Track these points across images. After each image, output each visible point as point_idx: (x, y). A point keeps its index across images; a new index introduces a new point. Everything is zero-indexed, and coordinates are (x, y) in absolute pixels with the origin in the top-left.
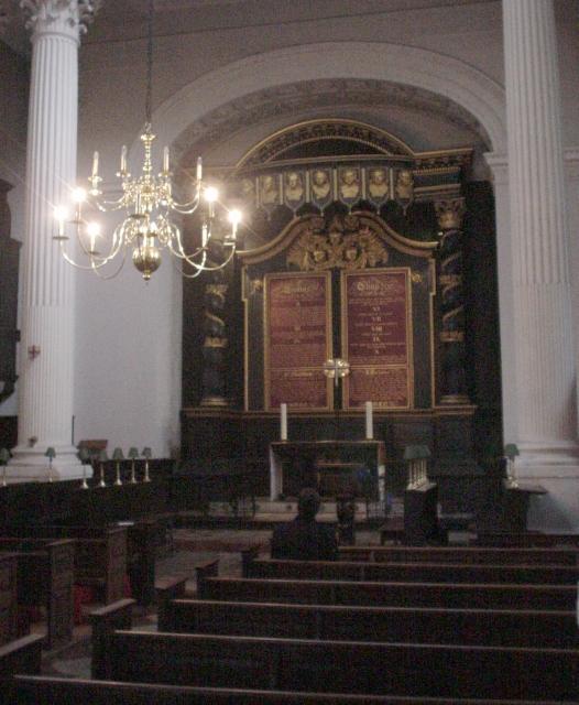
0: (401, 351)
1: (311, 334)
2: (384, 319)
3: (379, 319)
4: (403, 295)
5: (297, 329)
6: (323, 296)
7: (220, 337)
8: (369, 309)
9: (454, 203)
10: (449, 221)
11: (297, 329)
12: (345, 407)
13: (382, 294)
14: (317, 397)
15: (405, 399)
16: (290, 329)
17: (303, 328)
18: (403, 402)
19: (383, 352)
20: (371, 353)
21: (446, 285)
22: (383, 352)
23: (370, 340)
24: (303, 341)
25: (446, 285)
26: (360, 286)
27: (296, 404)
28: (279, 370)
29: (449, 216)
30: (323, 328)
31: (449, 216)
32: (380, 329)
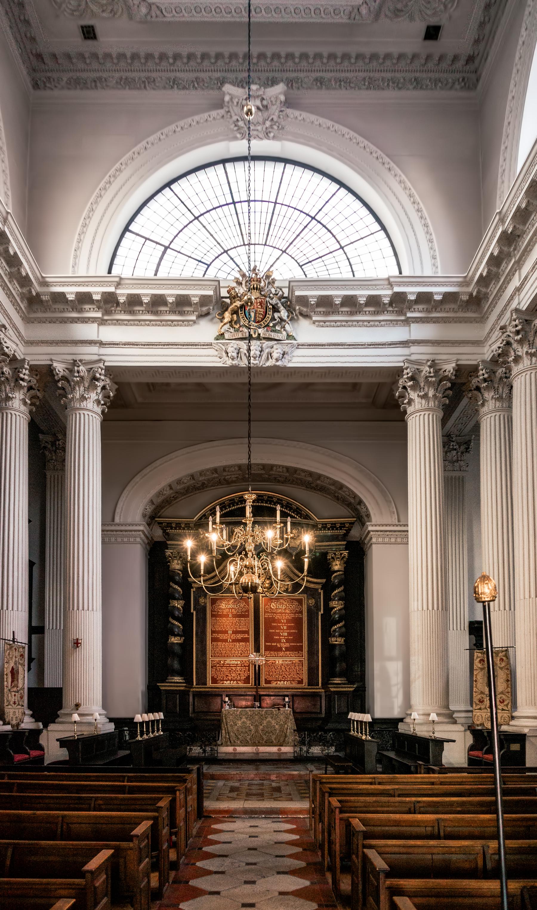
0: (300, 649)
1: (240, 636)
2: (289, 628)
3: (285, 628)
4: (301, 612)
5: (230, 632)
6: (248, 611)
7: (181, 636)
8: (279, 621)
9: (341, 554)
10: (337, 566)
11: (230, 632)
12: (263, 684)
13: (287, 611)
14: (243, 678)
15: (302, 680)
16: (226, 632)
17: (234, 632)
18: (300, 682)
19: (287, 649)
20: (280, 649)
21: (334, 608)
22: (287, 649)
23: (279, 641)
24: (234, 641)
25: (334, 608)
26: (273, 605)
27: (229, 682)
28: (217, 659)
29: (338, 563)
30: (247, 632)
31: (338, 563)
32: (286, 634)
